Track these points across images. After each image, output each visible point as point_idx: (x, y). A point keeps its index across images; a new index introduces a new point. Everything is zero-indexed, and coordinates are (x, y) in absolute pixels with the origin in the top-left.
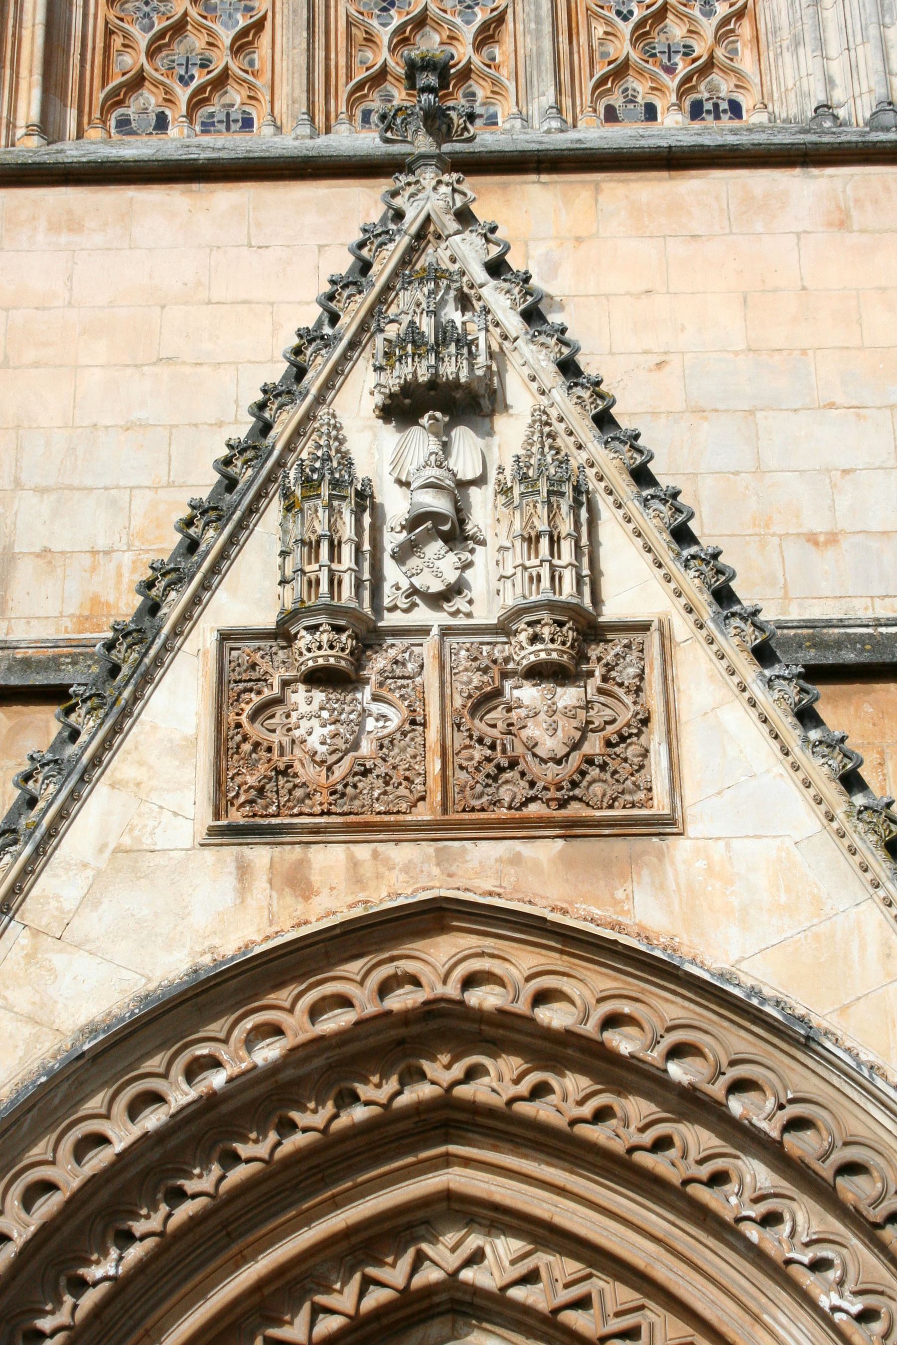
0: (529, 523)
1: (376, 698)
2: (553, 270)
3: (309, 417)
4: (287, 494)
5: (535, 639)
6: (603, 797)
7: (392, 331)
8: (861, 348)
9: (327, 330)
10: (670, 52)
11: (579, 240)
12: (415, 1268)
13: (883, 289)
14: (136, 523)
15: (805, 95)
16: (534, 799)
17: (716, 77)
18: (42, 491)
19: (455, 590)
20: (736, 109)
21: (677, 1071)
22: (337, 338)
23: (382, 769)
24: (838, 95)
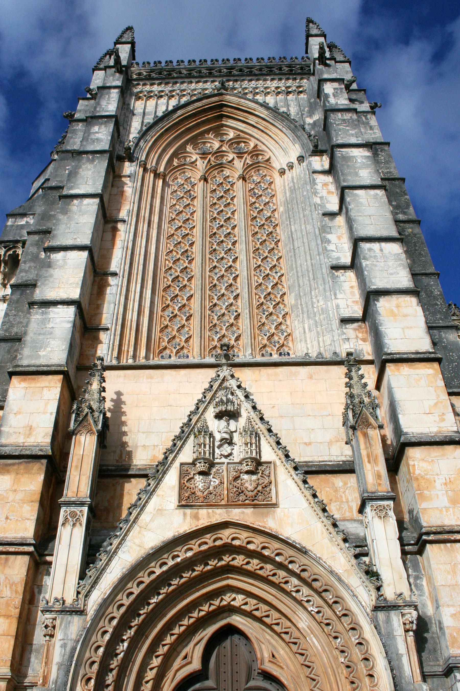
0: (246, 440)
1: (213, 478)
2: (251, 387)
3: (200, 418)
4: (195, 434)
5: (247, 465)
6: (261, 499)
7: (217, 400)
8: (315, 403)
9: (204, 400)
10: (275, 343)
11: (256, 381)
12: (221, 601)
13: (320, 391)
16: (247, 500)
17: (284, 347)
18: (143, 433)
19: (230, 454)
20: (288, 354)
21: (277, 559)
22: (206, 401)
23: (214, 493)
24: (310, 351)
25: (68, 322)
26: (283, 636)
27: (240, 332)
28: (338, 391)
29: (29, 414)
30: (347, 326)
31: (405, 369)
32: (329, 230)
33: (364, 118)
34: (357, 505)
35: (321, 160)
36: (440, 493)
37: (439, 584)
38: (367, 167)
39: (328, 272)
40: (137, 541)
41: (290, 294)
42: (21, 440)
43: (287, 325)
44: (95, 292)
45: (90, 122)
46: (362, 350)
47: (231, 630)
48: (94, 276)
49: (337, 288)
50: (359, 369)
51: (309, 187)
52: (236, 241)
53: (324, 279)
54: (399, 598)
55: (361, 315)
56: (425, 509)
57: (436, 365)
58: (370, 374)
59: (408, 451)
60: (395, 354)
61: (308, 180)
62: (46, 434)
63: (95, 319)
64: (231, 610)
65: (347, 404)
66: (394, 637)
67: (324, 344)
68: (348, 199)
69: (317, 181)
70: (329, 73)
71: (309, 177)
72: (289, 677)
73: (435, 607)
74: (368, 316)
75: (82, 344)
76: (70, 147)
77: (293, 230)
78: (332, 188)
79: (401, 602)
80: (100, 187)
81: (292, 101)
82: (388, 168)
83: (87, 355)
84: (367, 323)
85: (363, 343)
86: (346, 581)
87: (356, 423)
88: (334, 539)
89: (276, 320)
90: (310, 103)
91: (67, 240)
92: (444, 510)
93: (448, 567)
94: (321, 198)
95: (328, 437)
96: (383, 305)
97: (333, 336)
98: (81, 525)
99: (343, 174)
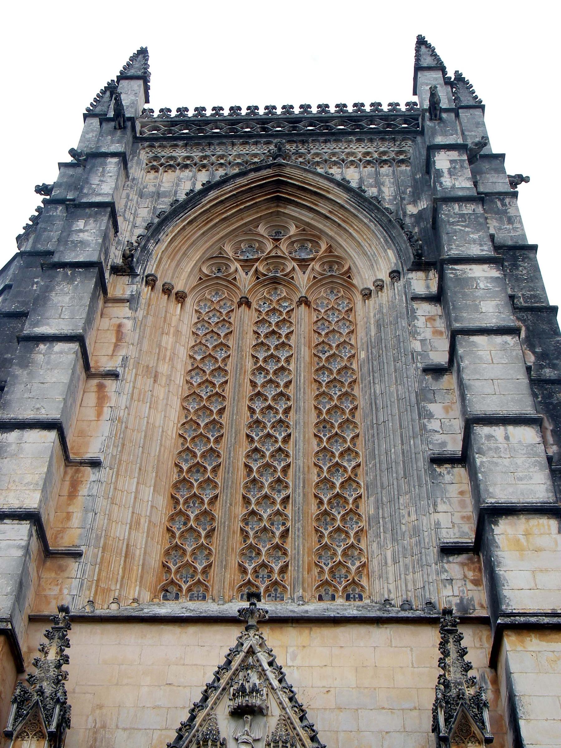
3: (208, 714)
4: (198, 743)
7: (235, 687)
8: (394, 688)
9: (216, 685)
13: (401, 667)
14: (154, 742)
18: (125, 729)
22: (219, 687)
24: (392, 596)
25: (19, 547)
27: (287, 559)
28: (431, 667)
30: (451, 559)
32: (431, 396)
33: (499, 204)
35: (427, 277)
38: (493, 297)
39: (426, 467)
41: (368, 497)
43: (361, 550)
44: (65, 492)
45: (72, 212)
46: (472, 599)
48: (66, 466)
49: (438, 494)
51: (404, 323)
52: (289, 408)
53: (419, 478)
61: (405, 310)
63: (62, 538)
65: (437, 699)
67: (414, 585)
68: (460, 351)
69: (419, 313)
70: (444, 134)
71: (407, 307)
74: (478, 550)
75: (39, 578)
76: (42, 245)
77: (378, 392)
78: (441, 325)
80: (81, 324)
81: (387, 175)
82: (533, 290)
83: (46, 596)
85: (475, 588)
87: (449, 733)
90: (415, 180)
91: (25, 410)
94: (423, 341)
96: (504, 531)
99: (454, 308)
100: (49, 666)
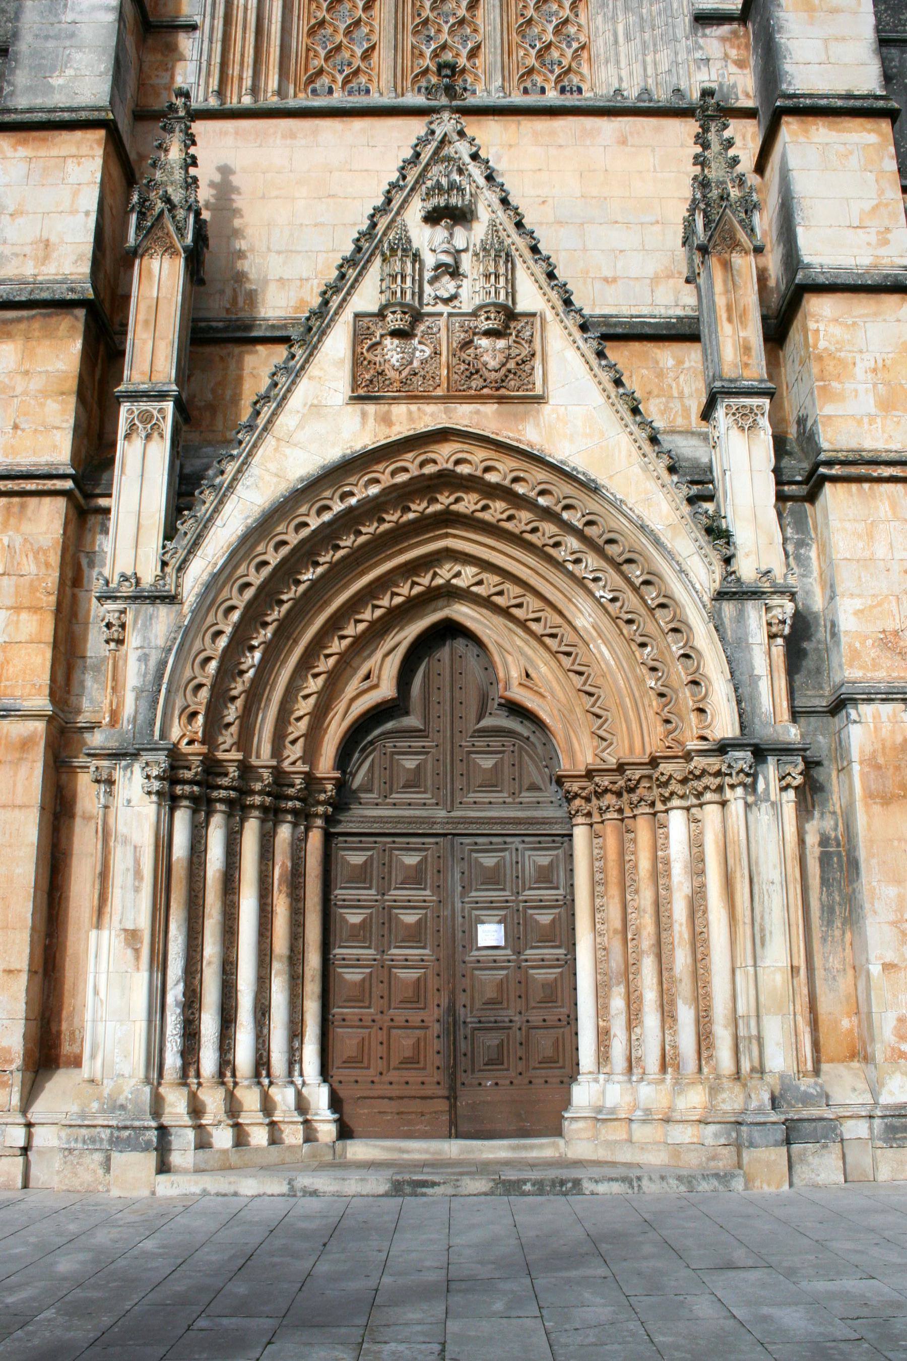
0: (486, 269)
1: (420, 343)
2: (499, 159)
3: (393, 221)
4: (383, 254)
5: (488, 319)
6: (514, 386)
7: (429, 184)
9: (401, 183)
10: (552, 64)
11: (510, 146)
12: (433, 579)
13: (640, 172)
14: (319, 267)
15: (609, 85)
17: (572, 75)
19: (454, 297)
20: (580, 90)
21: (542, 501)
22: (406, 186)
23: (422, 373)
24: (624, 85)
26: (548, 640)
27: (479, 38)
28: (679, 172)
29: (40, 216)
30: (708, 31)
31: (821, 132)
34: (699, 403)
36: (861, 388)
37: (839, 556)
40: (272, 467)
42: (28, 270)
43: (580, 26)
47: (451, 630)
50: (725, 126)
54: (764, 579)
55: (740, 7)
56: (829, 417)
57: (885, 125)
58: (745, 138)
59: (808, 302)
60: (803, 96)
62: (80, 258)
64: (450, 593)
65: (694, 200)
66: (748, 647)
67: (656, 69)
72: (556, 712)
73: (827, 597)
75: (141, 62)
79: (766, 586)
83: (152, 86)
84: (750, 25)
86: (669, 546)
87: (709, 241)
88: (651, 467)
89: (556, 13)
92: (866, 420)
93: (861, 527)
95: (652, 266)
97: (676, 54)
98: (162, 437)
100: (172, 168)
